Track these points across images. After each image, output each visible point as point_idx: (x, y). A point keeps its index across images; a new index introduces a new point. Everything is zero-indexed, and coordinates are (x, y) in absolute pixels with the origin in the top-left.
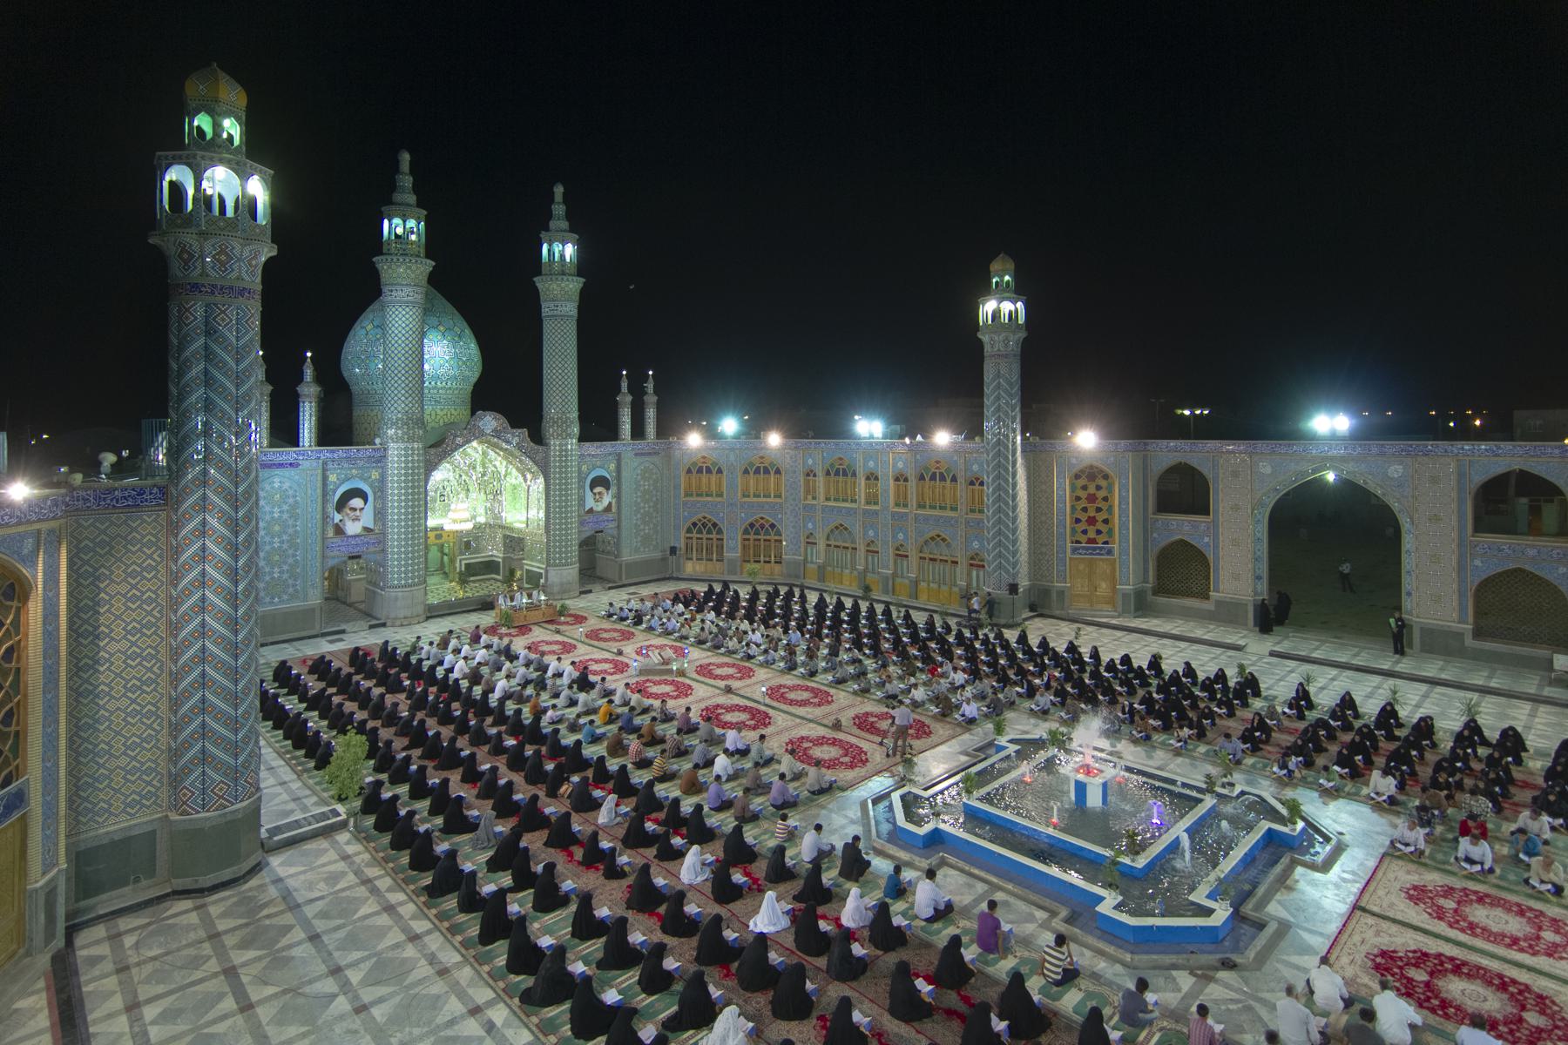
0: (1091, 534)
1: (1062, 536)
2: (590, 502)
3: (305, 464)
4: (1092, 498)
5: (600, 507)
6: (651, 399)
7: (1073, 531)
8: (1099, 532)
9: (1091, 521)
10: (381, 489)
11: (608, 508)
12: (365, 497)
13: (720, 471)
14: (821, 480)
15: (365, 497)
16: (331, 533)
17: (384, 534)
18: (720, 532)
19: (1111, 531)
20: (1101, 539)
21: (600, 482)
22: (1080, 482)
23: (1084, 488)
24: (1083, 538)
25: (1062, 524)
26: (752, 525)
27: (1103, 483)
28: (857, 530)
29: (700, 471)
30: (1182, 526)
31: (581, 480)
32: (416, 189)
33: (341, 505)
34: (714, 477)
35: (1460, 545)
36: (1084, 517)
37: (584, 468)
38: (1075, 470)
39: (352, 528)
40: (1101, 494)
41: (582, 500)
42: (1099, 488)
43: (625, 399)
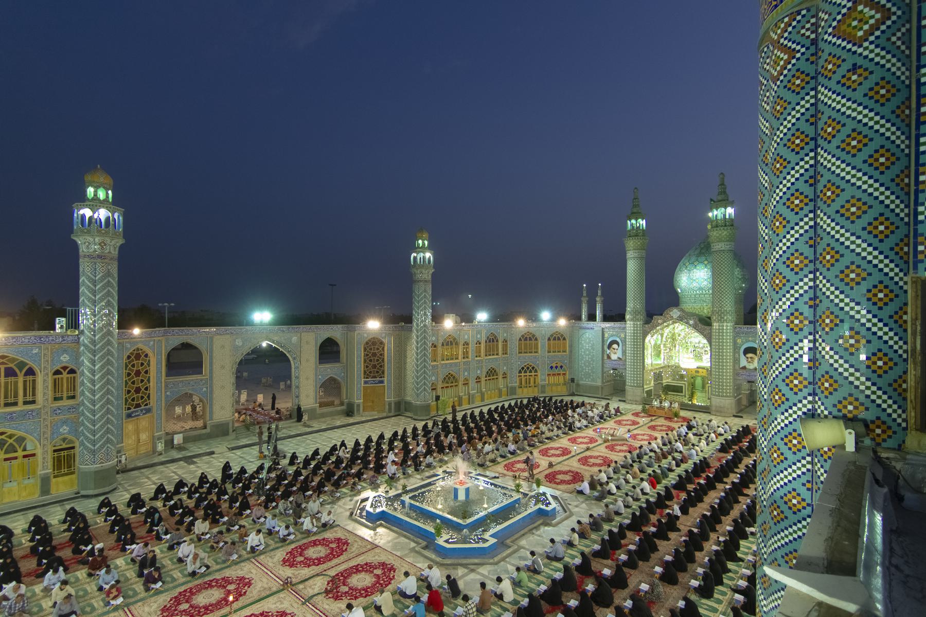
2: (743, 362)
3: (596, 329)
10: (624, 342)
21: (748, 351)
31: (736, 347)
33: (609, 347)
37: (739, 341)
39: (614, 357)
41: (736, 361)
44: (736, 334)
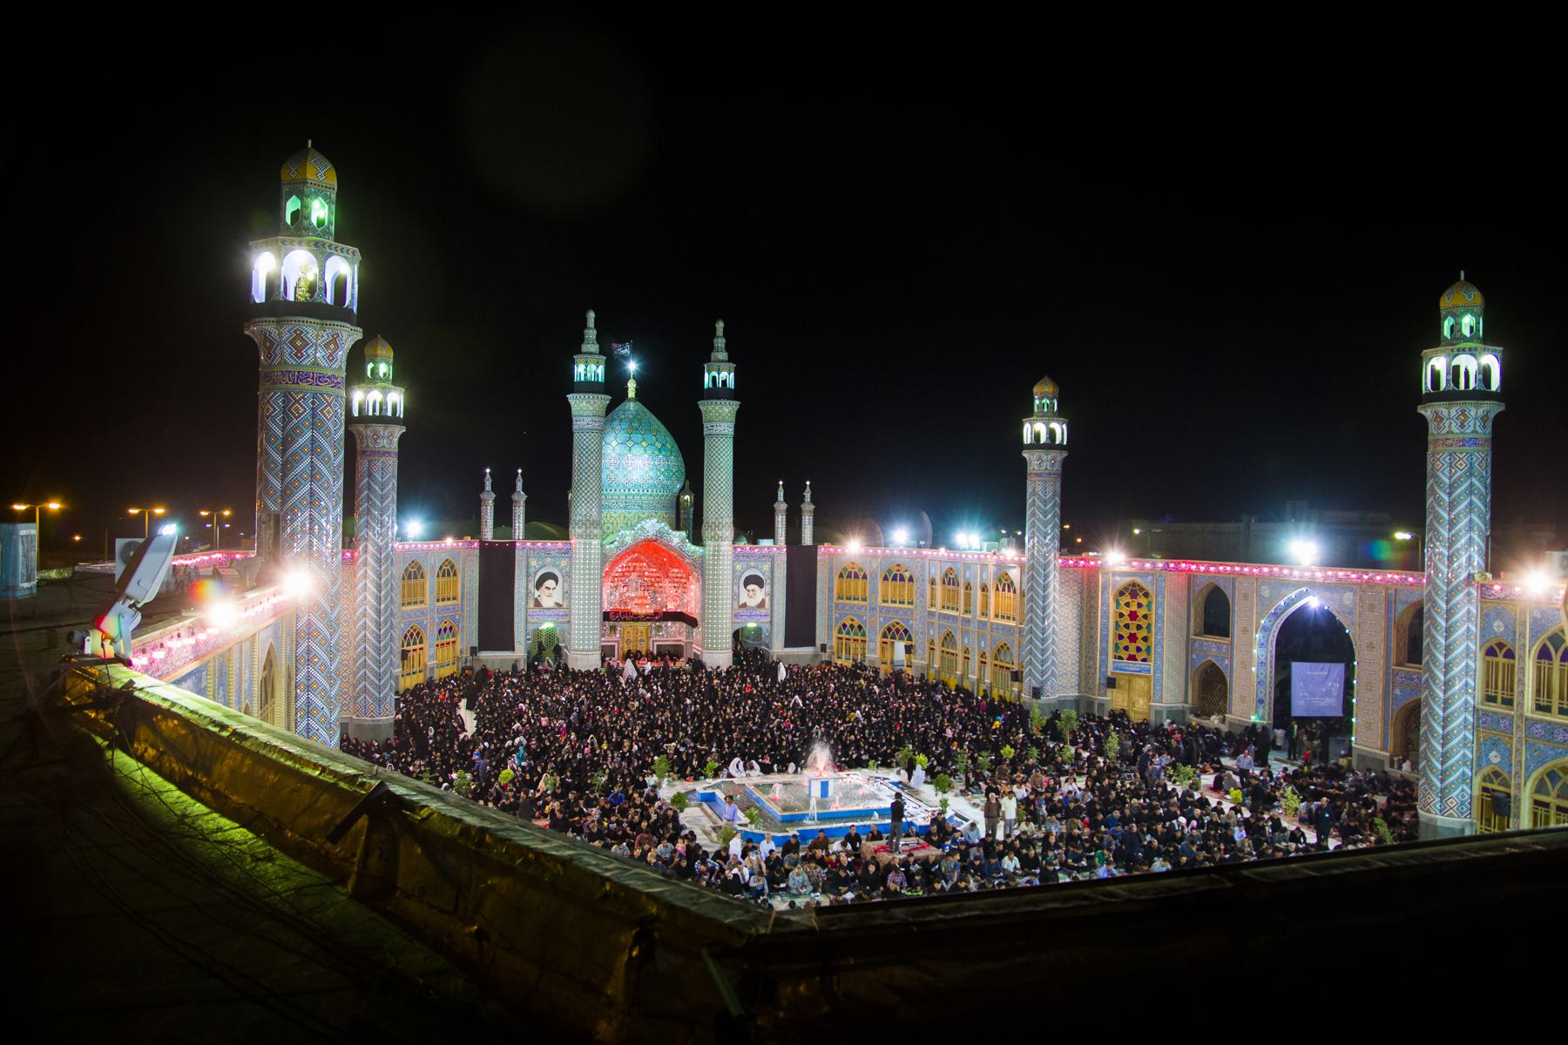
0: (1132, 651)
1: (1104, 651)
2: (744, 597)
4: (1133, 616)
5: (753, 603)
6: (808, 507)
7: (1117, 647)
8: (1139, 649)
9: (1133, 638)
11: (762, 604)
12: (555, 579)
13: (865, 577)
14: (939, 587)
15: (555, 579)
16: (531, 605)
17: (569, 608)
18: (864, 635)
19: (1148, 650)
20: (1140, 656)
21: (751, 580)
22: (1126, 598)
23: (1127, 604)
24: (1125, 654)
25: (1105, 638)
26: (889, 629)
27: (1144, 601)
28: (958, 637)
29: (849, 576)
30: (1212, 646)
31: (735, 578)
34: (860, 582)
35: (1386, 674)
36: (1125, 633)
37: (738, 567)
38: (1119, 586)
39: (547, 602)
40: (1141, 612)
41: (736, 596)
42: (1140, 605)
43: (781, 506)
44: (737, 557)
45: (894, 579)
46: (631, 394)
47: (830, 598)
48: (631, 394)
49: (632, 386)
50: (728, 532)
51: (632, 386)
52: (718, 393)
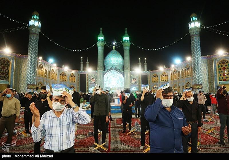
13: (157, 76)
32: (103, 33)
34: (157, 77)
44: (131, 74)
45: (164, 76)
46: (114, 48)
47: (151, 82)
48: (114, 48)
49: (114, 47)
50: (129, 69)
51: (114, 47)
52: (125, 42)
